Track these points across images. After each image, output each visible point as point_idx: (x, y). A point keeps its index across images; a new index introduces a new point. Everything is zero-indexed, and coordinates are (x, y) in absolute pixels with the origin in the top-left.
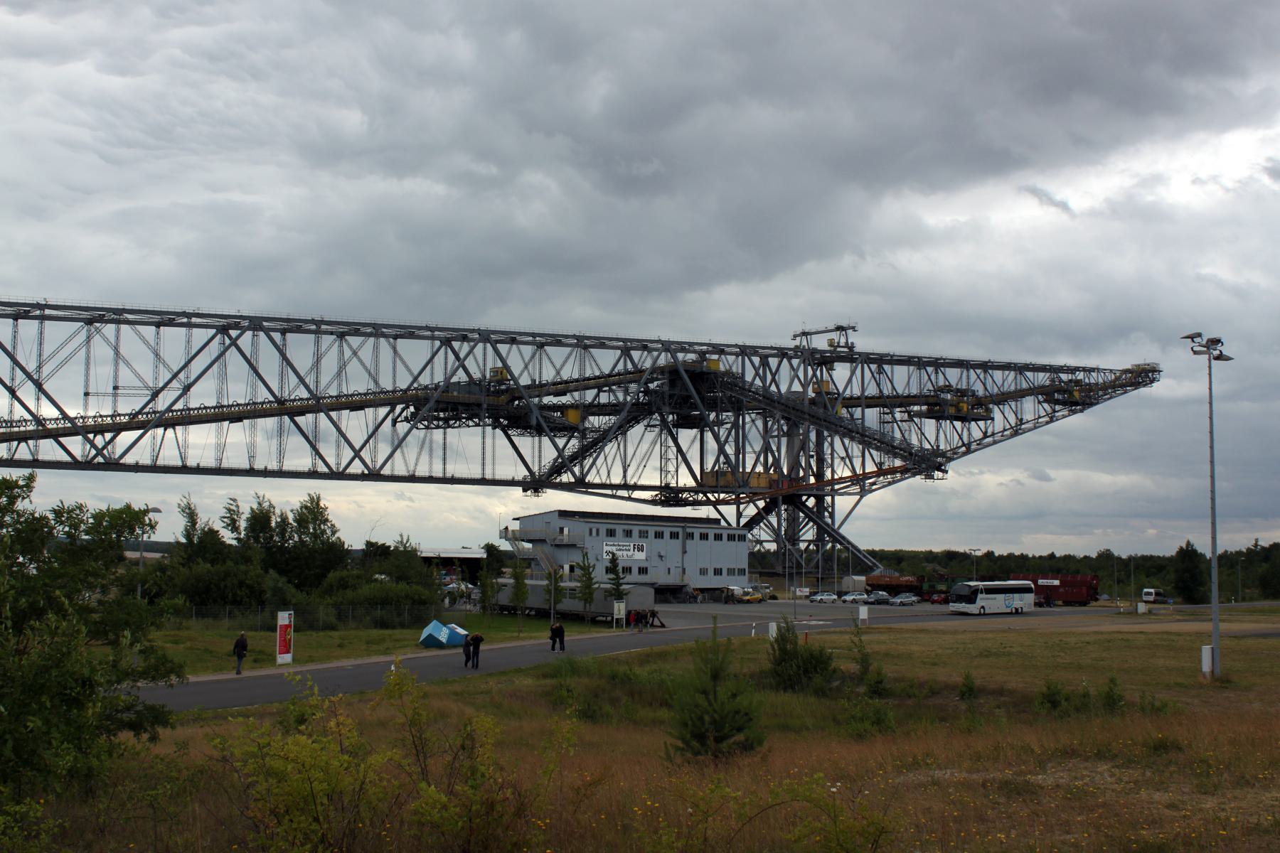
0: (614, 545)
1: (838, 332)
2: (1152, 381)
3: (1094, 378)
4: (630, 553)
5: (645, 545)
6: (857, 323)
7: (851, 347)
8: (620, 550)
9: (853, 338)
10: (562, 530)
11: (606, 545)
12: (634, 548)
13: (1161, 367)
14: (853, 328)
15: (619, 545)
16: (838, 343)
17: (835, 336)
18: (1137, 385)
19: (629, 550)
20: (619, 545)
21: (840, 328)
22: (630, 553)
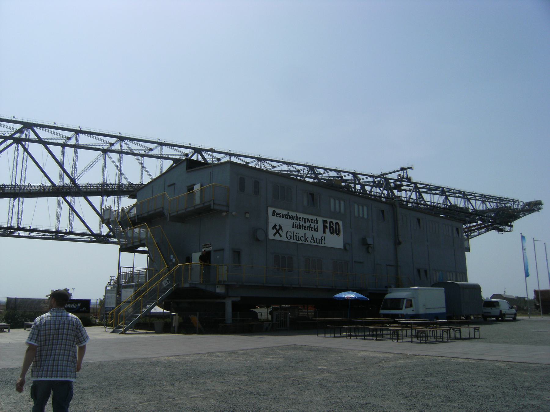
0: (288, 217)
1: (403, 171)
2: (540, 209)
3: (515, 206)
4: (318, 235)
5: (341, 223)
6: (412, 165)
7: (409, 179)
8: (300, 227)
9: (410, 173)
10: (191, 188)
11: (274, 214)
12: (324, 227)
13: (543, 202)
14: (411, 168)
15: (297, 218)
16: (403, 176)
17: (401, 173)
18: (533, 211)
19: (316, 230)
20: (297, 218)
21: (403, 169)
22: (318, 235)
